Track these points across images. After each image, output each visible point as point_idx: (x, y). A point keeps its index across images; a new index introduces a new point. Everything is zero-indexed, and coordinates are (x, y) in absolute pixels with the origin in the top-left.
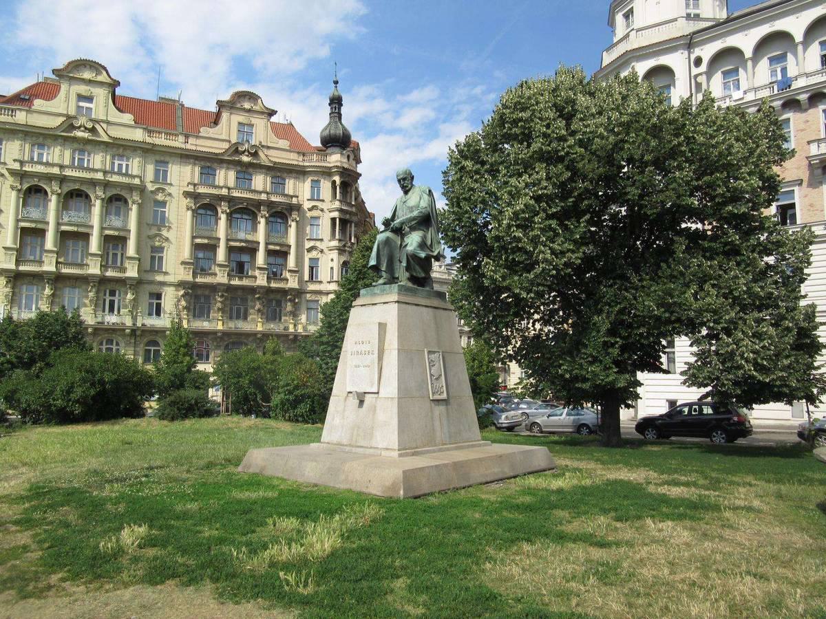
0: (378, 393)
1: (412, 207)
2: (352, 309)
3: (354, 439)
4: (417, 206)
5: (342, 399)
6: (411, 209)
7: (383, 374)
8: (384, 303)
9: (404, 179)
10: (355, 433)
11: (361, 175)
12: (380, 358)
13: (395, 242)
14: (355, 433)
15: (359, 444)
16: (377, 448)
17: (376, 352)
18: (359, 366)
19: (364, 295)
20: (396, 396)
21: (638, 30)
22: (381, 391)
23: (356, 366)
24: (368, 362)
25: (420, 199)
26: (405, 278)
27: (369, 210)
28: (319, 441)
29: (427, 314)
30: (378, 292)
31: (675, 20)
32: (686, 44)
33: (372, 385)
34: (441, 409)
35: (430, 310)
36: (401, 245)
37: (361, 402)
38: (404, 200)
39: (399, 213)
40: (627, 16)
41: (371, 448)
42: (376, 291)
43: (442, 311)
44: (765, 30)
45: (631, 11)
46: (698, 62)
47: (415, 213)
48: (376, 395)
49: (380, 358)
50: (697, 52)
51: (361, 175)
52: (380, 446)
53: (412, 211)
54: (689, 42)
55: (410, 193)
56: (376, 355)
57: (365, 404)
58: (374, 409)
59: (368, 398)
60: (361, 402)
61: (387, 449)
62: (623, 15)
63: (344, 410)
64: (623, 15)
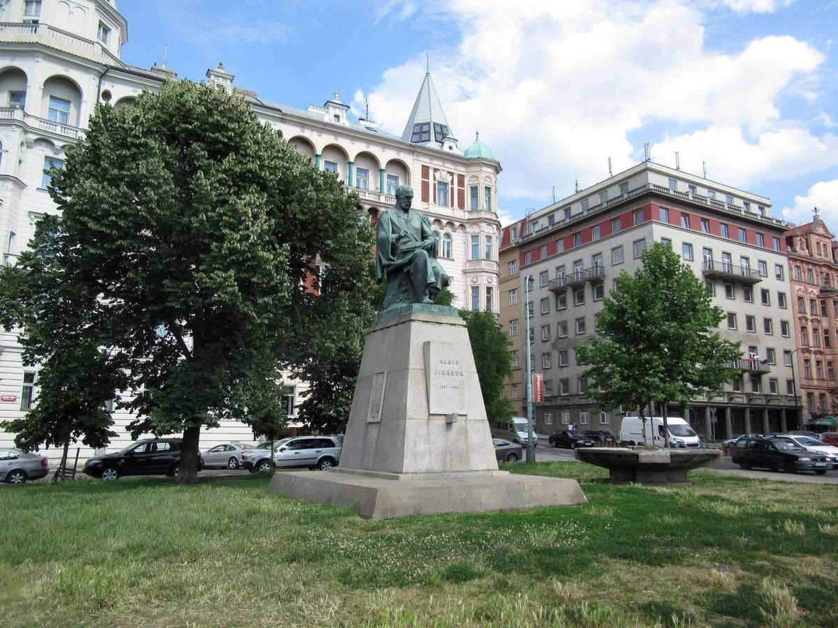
3: (448, 465)
10: (448, 457)
14: (448, 457)
20: (407, 421)
21: (50, 28)
24: (456, 384)
31: (92, 43)
32: (100, 72)
37: (449, 424)
41: (470, 471)
44: (60, 70)
46: (107, 95)
48: (464, 418)
50: (106, 86)
54: (104, 73)
57: (455, 426)
58: (465, 432)
60: (449, 424)
63: (428, 435)
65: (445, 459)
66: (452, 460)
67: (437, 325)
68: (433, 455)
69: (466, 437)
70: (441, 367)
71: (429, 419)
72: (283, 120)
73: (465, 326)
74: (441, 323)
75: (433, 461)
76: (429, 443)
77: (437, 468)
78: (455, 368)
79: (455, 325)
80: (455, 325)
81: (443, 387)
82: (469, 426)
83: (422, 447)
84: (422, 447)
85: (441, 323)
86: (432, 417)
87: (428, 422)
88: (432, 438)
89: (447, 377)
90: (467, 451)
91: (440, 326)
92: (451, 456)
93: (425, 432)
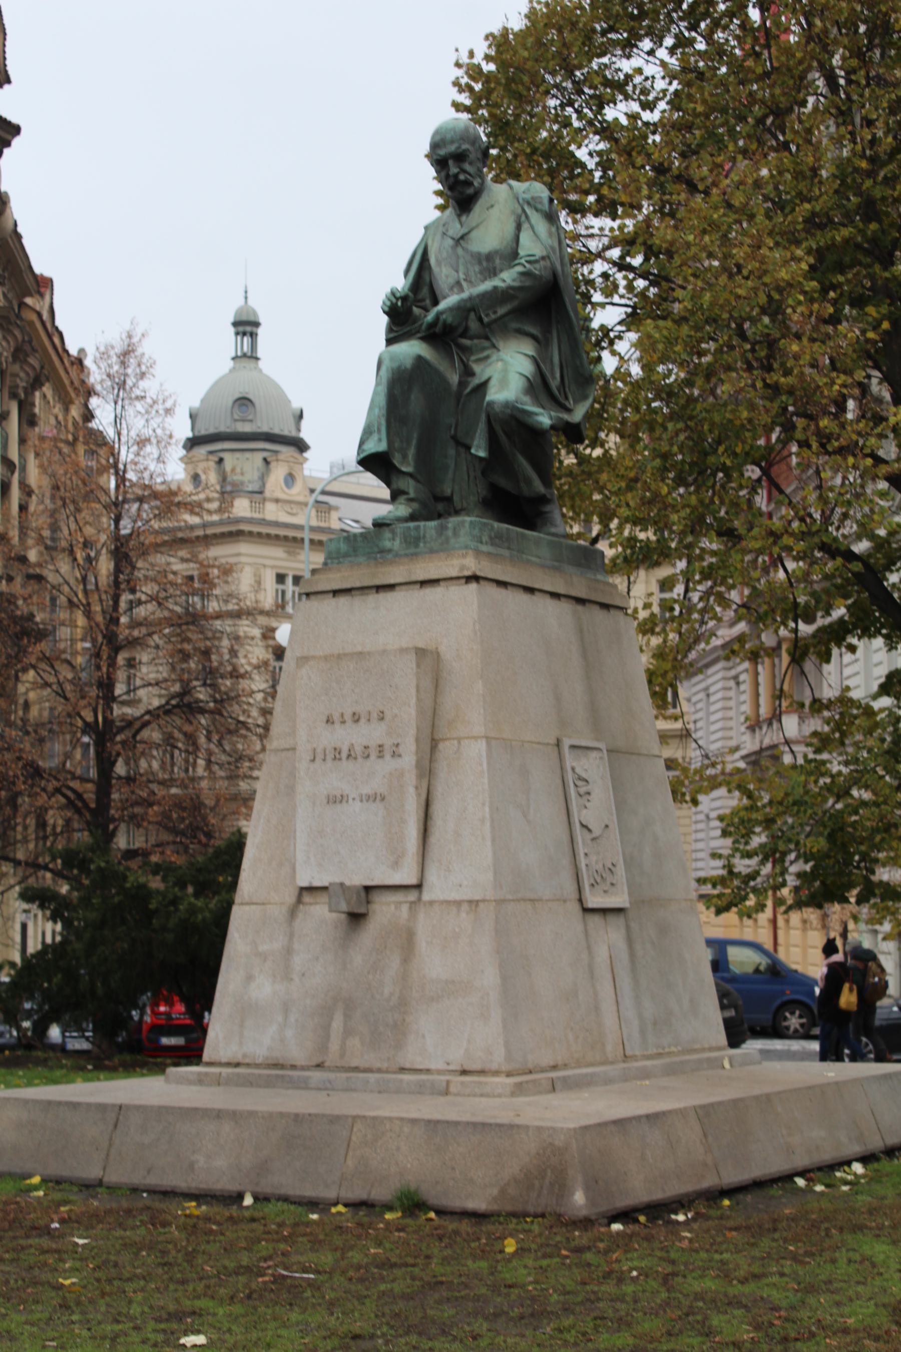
0: (419, 887)
1: (489, 257)
3: (334, 1046)
4: (512, 255)
5: (278, 912)
6: (489, 264)
8: (424, 583)
9: (460, 157)
10: (337, 1024)
11: (16, 130)
12: (427, 770)
13: (444, 380)
14: (337, 1024)
15: (355, 1063)
16: (428, 1071)
17: (409, 749)
22: (433, 877)
24: (376, 785)
25: (519, 227)
26: (473, 499)
27: (39, 268)
28: (192, 1053)
29: (555, 617)
30: (397, 544)
33: (396, 865)
34: (610, 938)
35: (565, 607)
36: (462, 384)
38: (456, 229)
39: (443, 274)
41: (402, 1070)
42: (387, 544)
43: (596, 610)
47: (508, 278)
48: (412, 896)
49: (427, 770)
51: (16, 130)
52: (436, 1064)
53: (493, 272)
55: (478, 208)
56: (408, 760)
58: (407, 943)
59: (385, 911)
60: (356, 918)
61: (464, 1072)
63: (289, 951)
65: (327, 1028)
66: (348, 1032)
67: (373, 598)
70: (328, 738)
71: (299, 901)
74: (391, 587)
76: (286, 975)
77: (297, 1053)
82: (424, 926)
83: (264, 989)
84: (264, 989)
85: (391, 587)
86: (307, 898)
87: (293, 912)
88: (298, 961)
89: (347, 766)
90: (403, 1004)
92: (347, 1016)
93: (278, 944)
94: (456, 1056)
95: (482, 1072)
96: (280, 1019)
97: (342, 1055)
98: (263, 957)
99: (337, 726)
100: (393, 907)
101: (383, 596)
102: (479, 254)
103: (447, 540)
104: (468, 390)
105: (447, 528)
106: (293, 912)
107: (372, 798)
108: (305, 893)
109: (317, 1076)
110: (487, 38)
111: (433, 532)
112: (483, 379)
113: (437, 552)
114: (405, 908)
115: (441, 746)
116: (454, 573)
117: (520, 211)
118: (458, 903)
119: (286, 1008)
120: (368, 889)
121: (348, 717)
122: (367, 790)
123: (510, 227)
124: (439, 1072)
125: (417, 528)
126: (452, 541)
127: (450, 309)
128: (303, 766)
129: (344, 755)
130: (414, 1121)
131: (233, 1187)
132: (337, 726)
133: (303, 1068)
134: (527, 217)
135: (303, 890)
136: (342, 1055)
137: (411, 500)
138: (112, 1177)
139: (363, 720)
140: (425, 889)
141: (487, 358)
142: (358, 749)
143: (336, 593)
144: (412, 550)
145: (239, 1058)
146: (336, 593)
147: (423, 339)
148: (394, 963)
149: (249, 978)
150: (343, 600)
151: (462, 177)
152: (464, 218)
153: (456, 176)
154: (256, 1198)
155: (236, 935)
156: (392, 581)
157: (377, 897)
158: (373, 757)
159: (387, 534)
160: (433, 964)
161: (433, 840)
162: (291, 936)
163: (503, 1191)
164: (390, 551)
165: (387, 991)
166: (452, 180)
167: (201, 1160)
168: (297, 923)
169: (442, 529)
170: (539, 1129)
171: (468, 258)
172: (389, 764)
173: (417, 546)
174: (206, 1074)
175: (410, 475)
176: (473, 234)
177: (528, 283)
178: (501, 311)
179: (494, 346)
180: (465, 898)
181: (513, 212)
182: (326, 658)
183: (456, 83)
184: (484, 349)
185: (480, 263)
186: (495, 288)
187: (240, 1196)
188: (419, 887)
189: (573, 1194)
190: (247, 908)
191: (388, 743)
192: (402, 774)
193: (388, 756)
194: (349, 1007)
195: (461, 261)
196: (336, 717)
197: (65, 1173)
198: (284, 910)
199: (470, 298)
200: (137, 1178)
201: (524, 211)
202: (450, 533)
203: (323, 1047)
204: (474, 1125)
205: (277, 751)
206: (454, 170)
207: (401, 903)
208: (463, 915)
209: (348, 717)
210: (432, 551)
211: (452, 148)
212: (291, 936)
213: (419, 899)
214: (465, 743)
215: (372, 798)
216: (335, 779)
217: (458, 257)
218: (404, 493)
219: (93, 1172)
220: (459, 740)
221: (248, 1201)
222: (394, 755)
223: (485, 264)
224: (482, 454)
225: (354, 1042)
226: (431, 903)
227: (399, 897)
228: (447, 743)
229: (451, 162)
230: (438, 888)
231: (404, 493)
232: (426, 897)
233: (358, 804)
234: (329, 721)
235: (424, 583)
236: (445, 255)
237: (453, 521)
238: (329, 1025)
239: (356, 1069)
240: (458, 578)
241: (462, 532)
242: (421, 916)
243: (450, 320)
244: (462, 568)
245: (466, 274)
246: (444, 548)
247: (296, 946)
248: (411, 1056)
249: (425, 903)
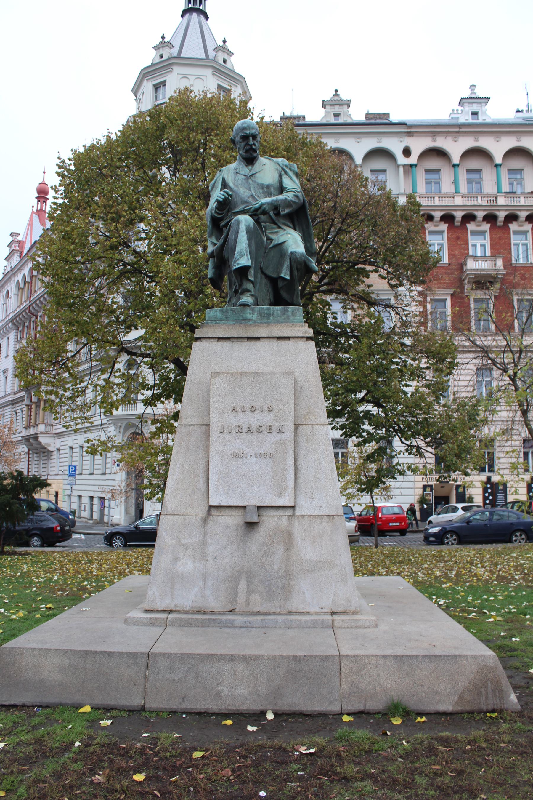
1: (268, 187)
2: (196, 345)
3: (241, 599)
7: (302, 470)
8: (279, 338)
10: (242, 586)
14: (242, 586)
17: (290, 428)
18: (243, 455)
19: (217, 320)
23: (236, 456)
24: (267, 448)
25: (281, 177)
30: (255, 316)
33: (280, 494)
40: (157, 87)
42: (249, 316)
45: (164, 83)
48: (289, 512)
56: (289, 434)
58: (289, 540)
59: (270, 520)
60: (251, 525)
62: (154, 85)
63: (204, 543)
64: (154, 85)
66: (250, 592)
67: (246, 344)
68: (209, 583)
69: (287, 550)
70: (232, 420)
71: (209, 514)
72: (410, 134)
73: (309, 339)
74: (258, 339)
75: (208, 592)
78: (267, 419)
79: (288, 338)
80: (288, 338)
81: (236, 456)
82: (298, 529)
83: (187, 565)
84: (187, 565)
85: (258, 339)
86: (214, 512)
87: (205, 521)
88: (211, 549)
90: (288, 574)
91: (258, 343)
92: (249, 582)
93: (196, 539)
94: (327, 604)
95: (344, 613)
96: (200, 584)
97: (248, 605)
98: (186, 547)
99: (240, 413)
100: (276, 518)
101: (252, 343)
102: (262, 184)
103: (288, 317)
104: (271, 245)
105: (288, 311)
106: (205, 521)
107: (265, 456)
108: (212, 509)
109: (238, 619)
110: (72, 150)
111: (279, 312)
112: (280, 242)
113: (282, 322)
114: (285, 519)
115: (300, 428)
116: (300, 335)
117: (280, 169)
118: (321, 517)
119: (204, 578)
120: (259, 507)
121: (247, 408)
122: (260, 451)
123: (276, 176)
124: (317, 613)
125: (270, 309)
126: (292, 318)
127: (268, 203)
128: (214, 435)
129: (245, 430)
130: (385, 657)
131: (257, 707)
132: (240, 413)
133: (220, 613)
134: (286, 173)
135: (211, 507)
136: (248, 605)
137: (252, 295)
138: (151, 704)
139: (258, 411)
140: (297, 508)
141: (277, 232)
142: (254, 428)
143: (219, 339)
144: (265, 321)
145: (172, 607)
146: (219, 339)
147: (251, 216)
148: (280, 551)
149: (176, 559)
150: (226, 343)
151: (254, 147)
152: (250, 167)
153: (251, 145)
154: (276, 714)
155: (164, 533)
156: (259, 336)
157: (264, 512)
158: (264, 432)
159: (248, 310)
160: (306, 551)
161: (300, 481)
162: (205, 534)
163: (461, 697)
164: (250, 320)
165: (276, 568)
166: (248, 147)
167: (225, 691)
168: (209, 527)
169: (285, 312)
170: (474, 657)
171: (256, 185)
172: (276, 437)
173: (268, 319)
174: (156, 619)
175: (252, 282)
176: (257, 175)
177: (297, 201)
178: (287, 211)
179: (280, 227)
180: (324, 514)
181: (277, 169)
182: (232, 374)
183: (57, 165)
184: (273, 228)
185: (263, 188)
186: (286, 199)
187: (263, 713)
188: (293, 507)
189: (509, 696)
190: (172, 517)
191: (275, 424)
192: (284, 443)
193: (275, 433)
194: (250, 576)
195: (251, 186)
196: (238, 408)
197: (111, 702)
198: (199, 518)
199: (277, 200)
200: (174, 705)
201: (283, 169)
202: (290, 314)
203: (234, 600)
204: (429, 657)
205: (185, 425)
206: (251, 142)
207: (282, 516)
208: (325, 524)
209: (247, 408)
210: (278, 322)
211: (253, 131)
212: (205, 534)
213: (294, 514)
214: (316, 427)
215: (265, 456)
216: (237, 444)
217: (250, 184)
218: (249, 291)
219: (136, 701)
220: (312, 425)
221: (270, 716)
222: (280, 432)
223: (265, 189)
224: (288, 277)
225: (255, 598)
226: (302, 516)
227: (280, 512)
228: (305, 427)
229: (251, 138)
230: (305, 507)
231: (249, 291)
232: (298, 513)
233: (254, 459)
234: (234, 410)
235: (279, 338)
236: (239, 182)
237: (291, 308)
238: (237, 587)
239: (257, 613)
240: (302, 337)
241: (298, 314)
242: (296, 524)
243: (267, 209)
244: (305, 332)
245: (255, 192)
246: (286, 321)
247: (209, 540)
248: (295, 604)
249: (298, 516)
